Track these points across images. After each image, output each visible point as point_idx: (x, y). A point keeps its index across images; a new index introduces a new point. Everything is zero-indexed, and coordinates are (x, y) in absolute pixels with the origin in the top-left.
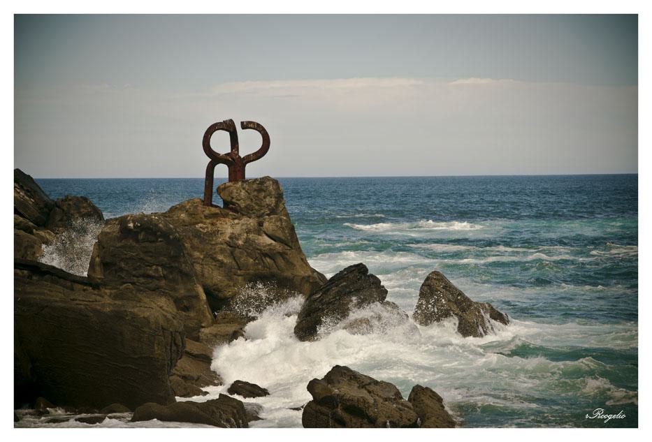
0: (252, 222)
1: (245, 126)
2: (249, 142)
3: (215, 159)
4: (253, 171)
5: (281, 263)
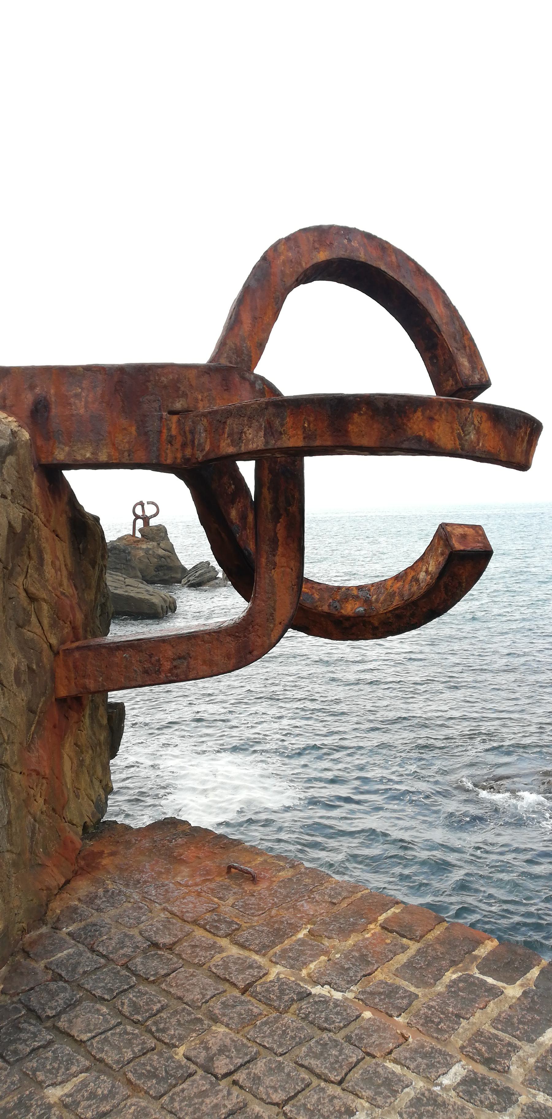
0: (155, 544)
1: (148, 503)
2: (150, 510)
3: (137, 517)
4: (153, 522)
5: (169, 560)
